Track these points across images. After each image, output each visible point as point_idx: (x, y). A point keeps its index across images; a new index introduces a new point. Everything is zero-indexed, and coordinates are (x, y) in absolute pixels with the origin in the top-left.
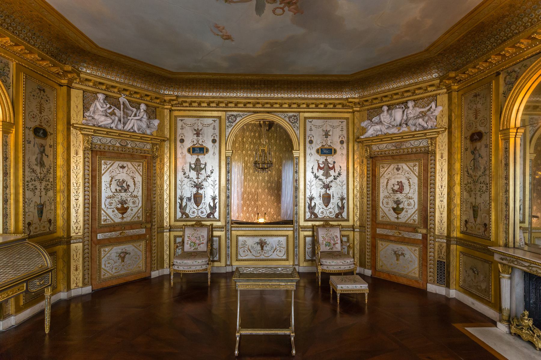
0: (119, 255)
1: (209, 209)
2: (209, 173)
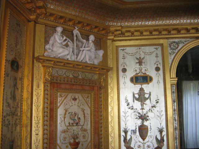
2: (154, 103)
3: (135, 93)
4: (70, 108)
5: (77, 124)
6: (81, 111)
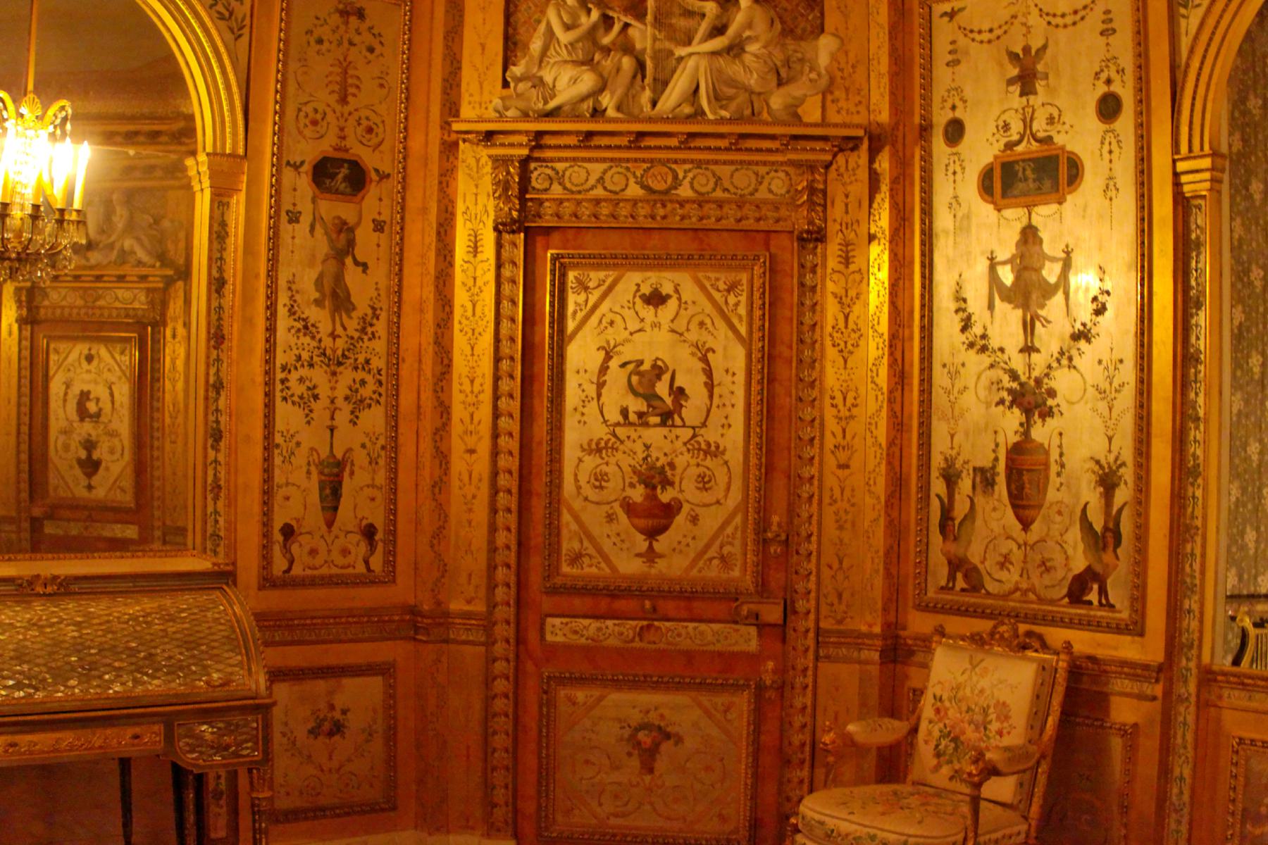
0: (633, 737)
1: (1081, 547)
2: (1084, 313)
3: (1002, 255)
4: (627, 341)
6: (693, 354)
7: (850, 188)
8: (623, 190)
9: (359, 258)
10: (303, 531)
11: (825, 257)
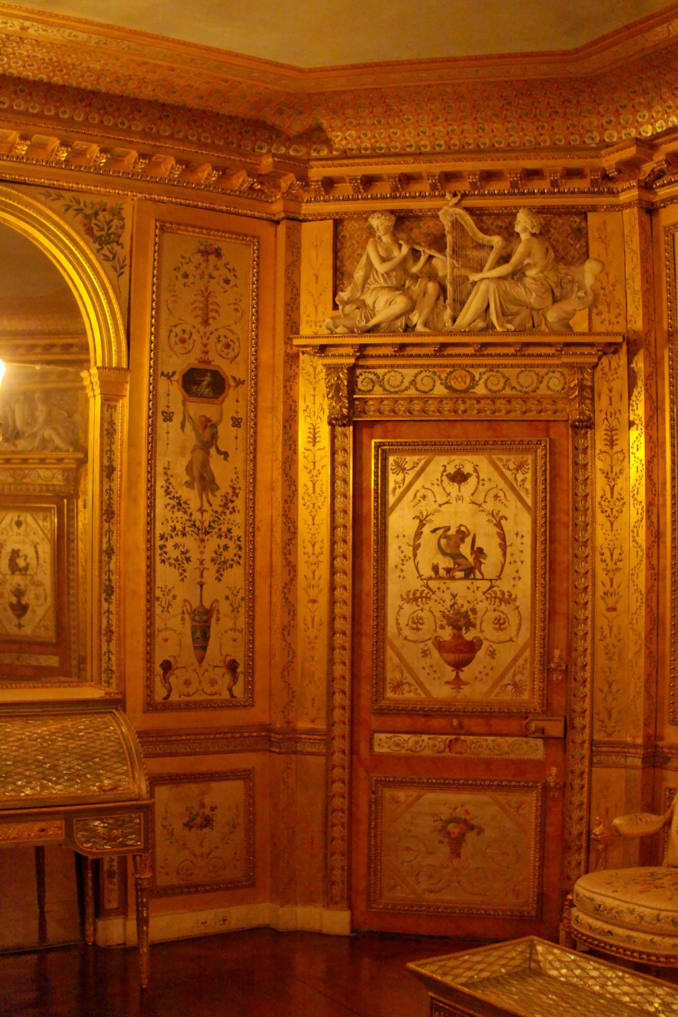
0: (444, 828)
4: (437, 511)
5: (469, 573)
6: (489, 521)
7: (612, 384)
8: (431, 390)
9: (222, 449)
10: (179, 666)
11: (594, 441)
